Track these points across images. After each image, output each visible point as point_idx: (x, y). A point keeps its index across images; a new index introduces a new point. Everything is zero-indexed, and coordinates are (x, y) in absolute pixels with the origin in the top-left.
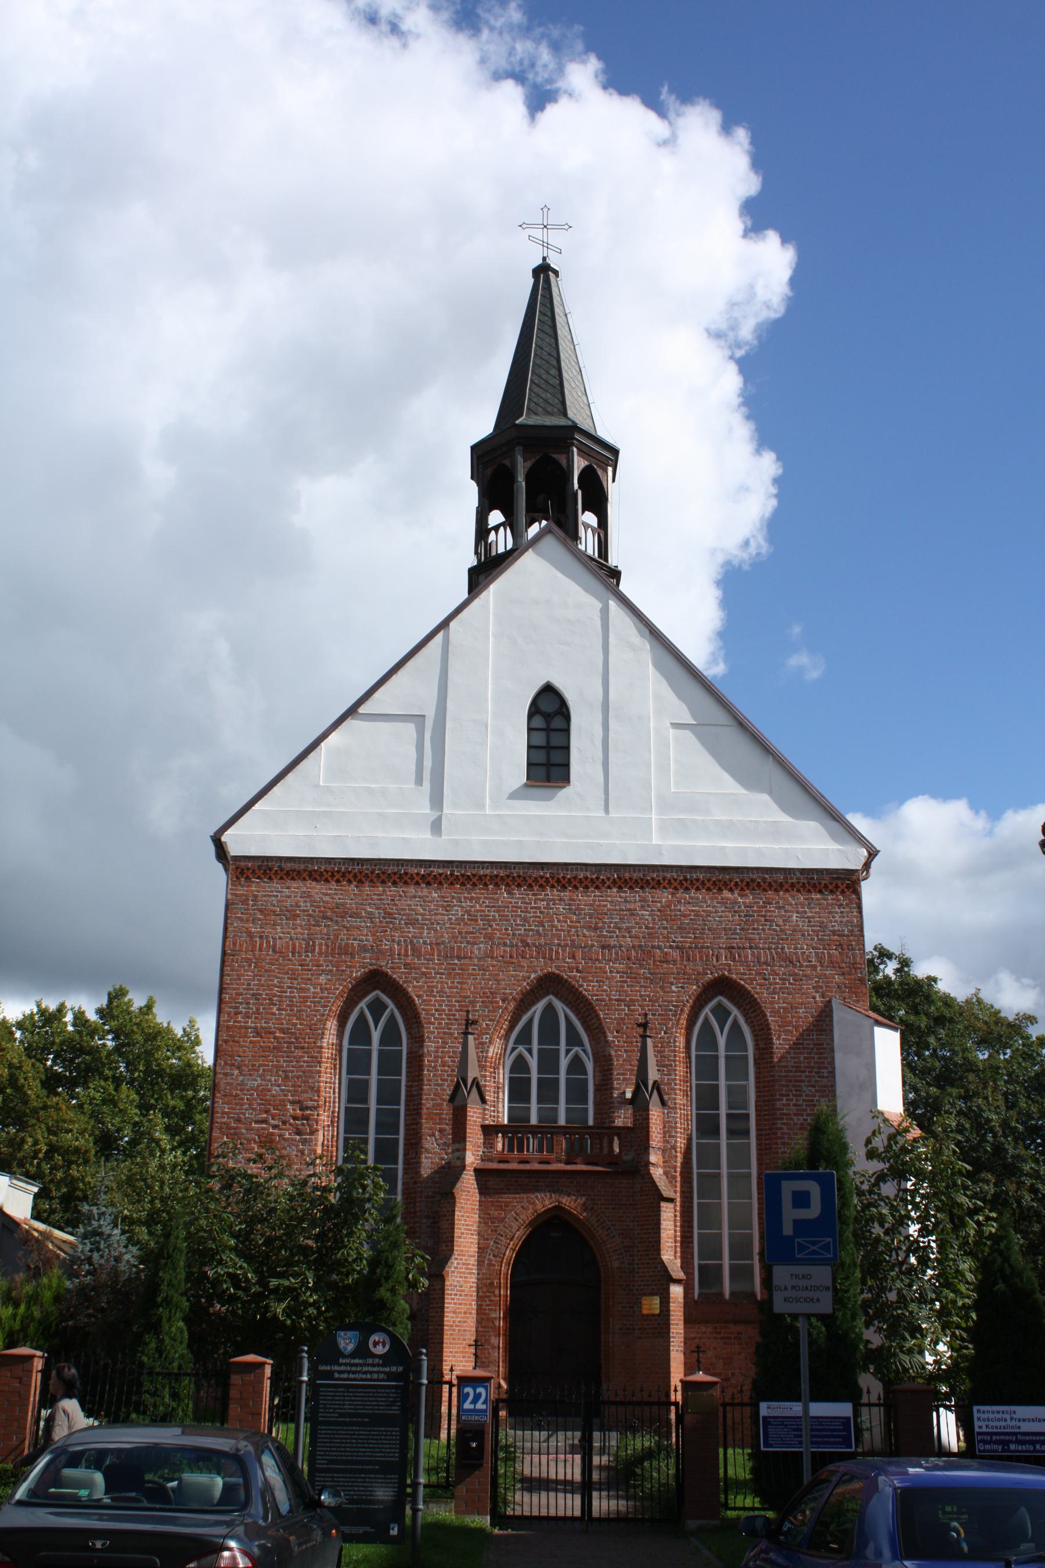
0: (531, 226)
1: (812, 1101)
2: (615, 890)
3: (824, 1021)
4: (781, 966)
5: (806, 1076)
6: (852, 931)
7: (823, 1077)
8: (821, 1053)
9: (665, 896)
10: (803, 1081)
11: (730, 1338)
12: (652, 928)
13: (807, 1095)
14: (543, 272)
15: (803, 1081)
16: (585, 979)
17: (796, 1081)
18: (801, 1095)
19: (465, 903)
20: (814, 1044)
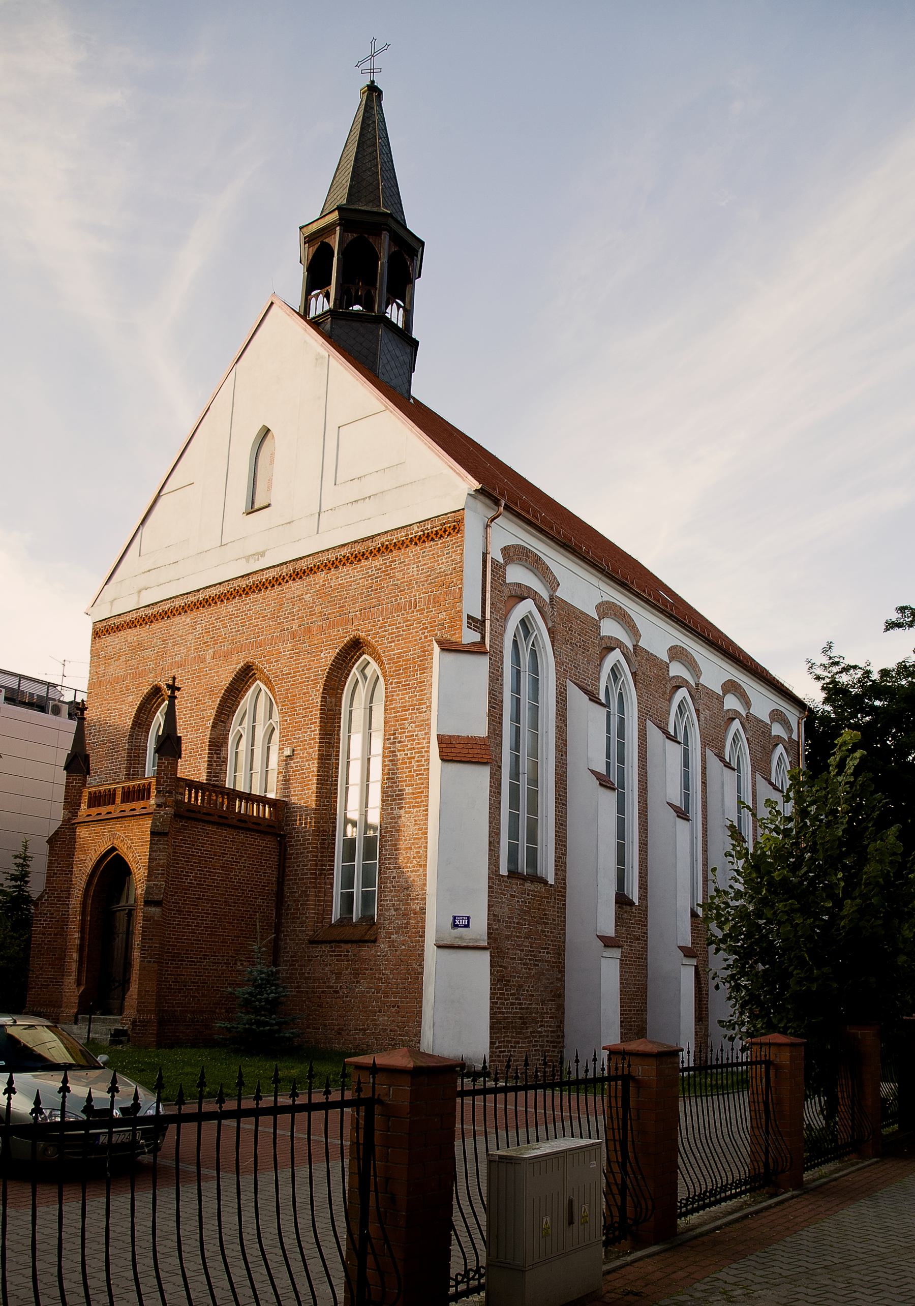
0: (363, 62)
1: (412, 736)
2: (290, 582)
3: (426, 660)
4: (398, 616)
5: (410, 714)
6: (455, 569)
7: (422, 712)
8: (422, 691)
9: (321, 576)
10: (406, 719)
11: (341, 956)
12: (312, 607)
13: (409, 732)
14: (373, 92)
15: (406, 719)
16: (268, 662)
17: (402, 720)
18: (404, 732)
19: (204, 616)
20: (418, 683)
